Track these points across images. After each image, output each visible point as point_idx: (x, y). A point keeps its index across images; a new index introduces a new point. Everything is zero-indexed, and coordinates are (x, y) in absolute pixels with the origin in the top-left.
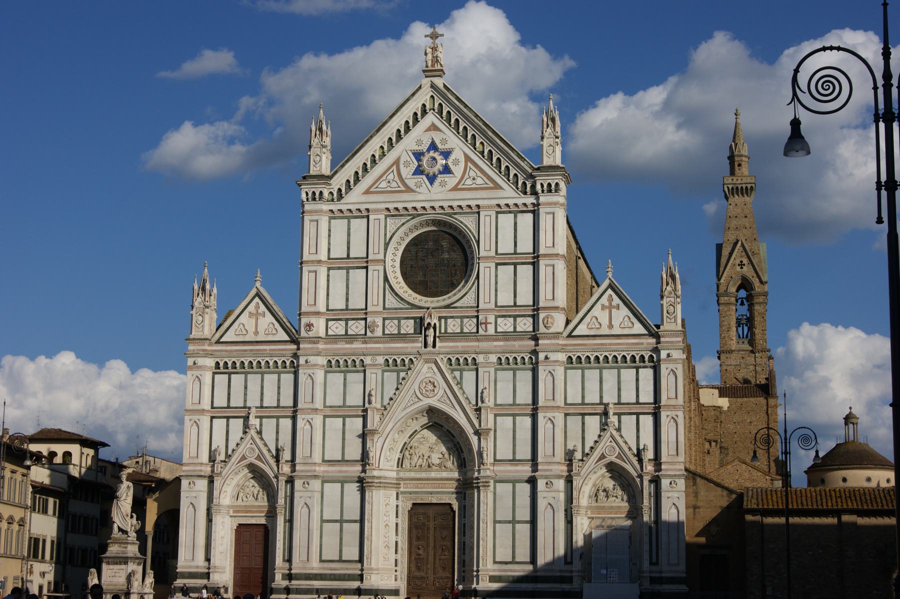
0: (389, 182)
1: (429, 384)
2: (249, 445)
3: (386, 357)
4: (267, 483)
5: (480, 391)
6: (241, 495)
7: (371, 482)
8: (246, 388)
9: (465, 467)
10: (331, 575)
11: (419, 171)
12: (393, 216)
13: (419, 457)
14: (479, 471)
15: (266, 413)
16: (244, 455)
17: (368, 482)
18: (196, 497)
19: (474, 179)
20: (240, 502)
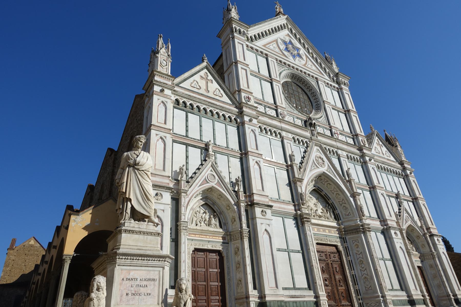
0: (274, 47)
1: (319, 159)
2: (209, 172)
3: (293, 136)
4: (219, 211)
5: (345, 172)
6: (195, 219)
7: (308, 218)
8: (201, 126)
9: (341, 220)
10: (293, 302)
11: (287, 49)
12: (278, 63)
13: (311, 210)
14: (361, 220)
15: (219, 149)
16: (205, 179)
17: (306, 218)
18: (163, 210)
19: (311, 66)
20: (193, 226)
